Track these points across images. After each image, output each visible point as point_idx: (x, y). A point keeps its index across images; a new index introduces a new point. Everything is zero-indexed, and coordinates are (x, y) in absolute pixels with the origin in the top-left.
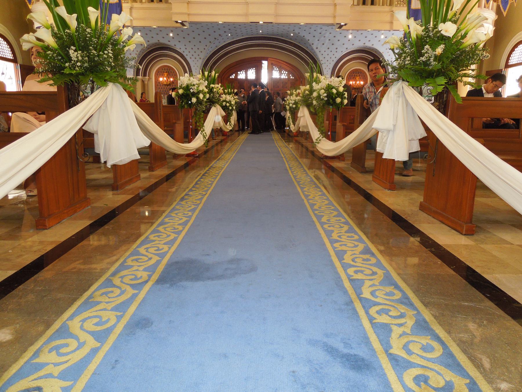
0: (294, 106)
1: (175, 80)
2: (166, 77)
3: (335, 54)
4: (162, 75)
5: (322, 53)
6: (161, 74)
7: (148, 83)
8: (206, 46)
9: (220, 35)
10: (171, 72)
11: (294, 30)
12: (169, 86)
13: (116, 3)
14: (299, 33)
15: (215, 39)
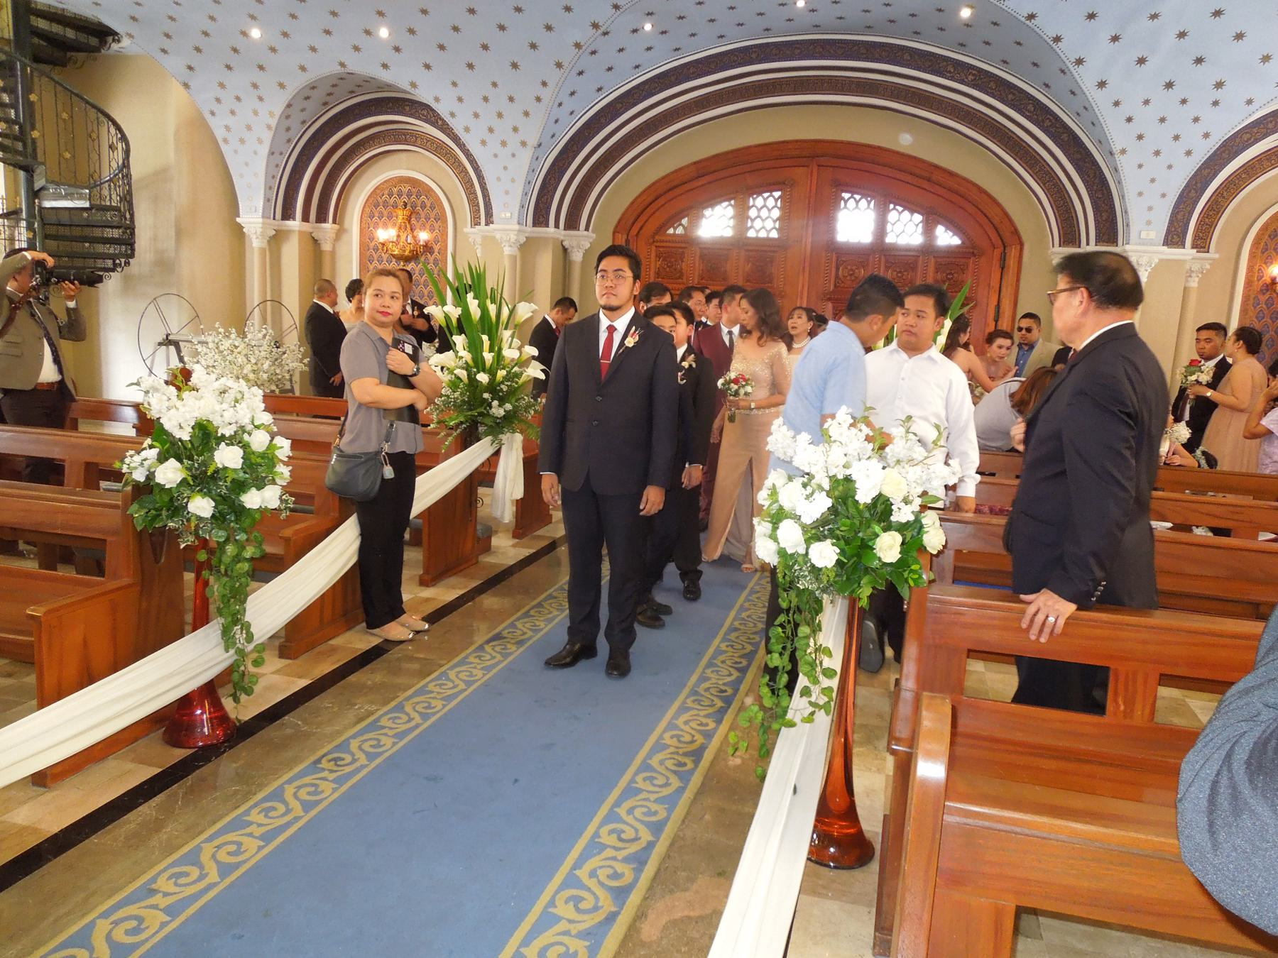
1: (436, 241)
3: (1208, 114)
4: (390, 217)
6: (385, 213)
7: (334, 245)
8: (544, 84)
10: (423, 206)
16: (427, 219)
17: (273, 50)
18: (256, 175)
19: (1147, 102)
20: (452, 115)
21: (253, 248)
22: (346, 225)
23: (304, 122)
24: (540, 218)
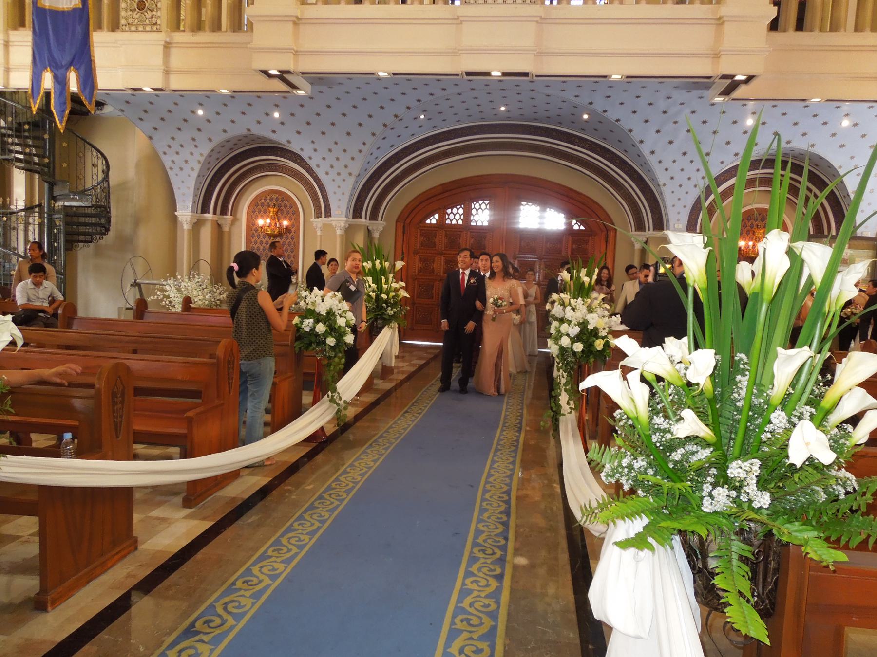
0: (578, 347)
1: (293, 226)
4: (265, 212)
5: (665, 165)
6: (262, 210)
7: (230, 228)
8: (364, 144)
10: (285, 206)
11: (591, 103)
14: (605, 111)
15: (385, 125)
16: (288, 213)
17: (209, 121)
19: (674, 161)
20: (310, 158)
21: (183, 230)
22: (238, 216)
23: (218, 159)
24: (357, 212)
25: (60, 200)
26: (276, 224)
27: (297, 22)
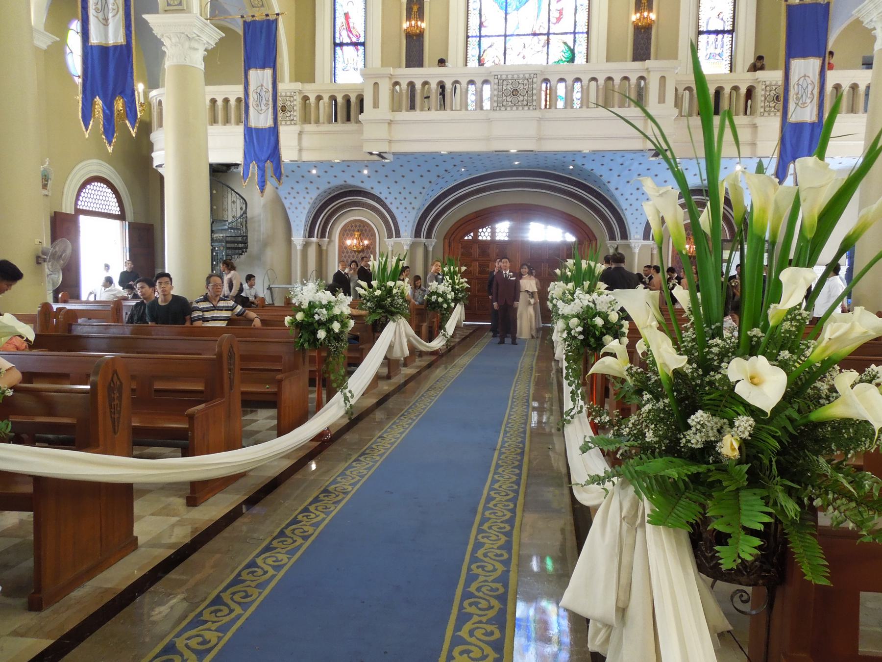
1: (371, 244)
2: (357, 239)
4: (351, 235)
6: (349, 234)
7: (327, 247)
8: (424, 188)
9: (446, 171)
11: (574, 161)
12: (361, 254)
13: (270, 128)
14: (583, 165)
15: (438, 176)
16: (368, 236)
17: (319, 177)
18: (301, 221)
24: (417, 234)
25: (217, 233)
26: (359, 243)
27: (390, 123)
